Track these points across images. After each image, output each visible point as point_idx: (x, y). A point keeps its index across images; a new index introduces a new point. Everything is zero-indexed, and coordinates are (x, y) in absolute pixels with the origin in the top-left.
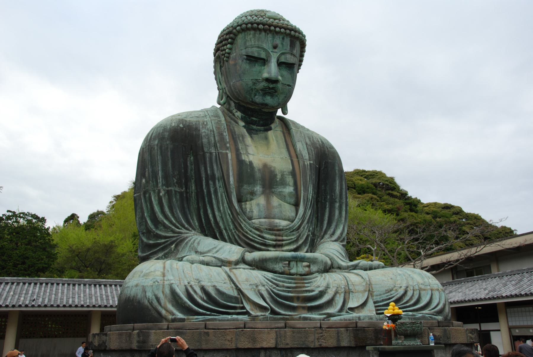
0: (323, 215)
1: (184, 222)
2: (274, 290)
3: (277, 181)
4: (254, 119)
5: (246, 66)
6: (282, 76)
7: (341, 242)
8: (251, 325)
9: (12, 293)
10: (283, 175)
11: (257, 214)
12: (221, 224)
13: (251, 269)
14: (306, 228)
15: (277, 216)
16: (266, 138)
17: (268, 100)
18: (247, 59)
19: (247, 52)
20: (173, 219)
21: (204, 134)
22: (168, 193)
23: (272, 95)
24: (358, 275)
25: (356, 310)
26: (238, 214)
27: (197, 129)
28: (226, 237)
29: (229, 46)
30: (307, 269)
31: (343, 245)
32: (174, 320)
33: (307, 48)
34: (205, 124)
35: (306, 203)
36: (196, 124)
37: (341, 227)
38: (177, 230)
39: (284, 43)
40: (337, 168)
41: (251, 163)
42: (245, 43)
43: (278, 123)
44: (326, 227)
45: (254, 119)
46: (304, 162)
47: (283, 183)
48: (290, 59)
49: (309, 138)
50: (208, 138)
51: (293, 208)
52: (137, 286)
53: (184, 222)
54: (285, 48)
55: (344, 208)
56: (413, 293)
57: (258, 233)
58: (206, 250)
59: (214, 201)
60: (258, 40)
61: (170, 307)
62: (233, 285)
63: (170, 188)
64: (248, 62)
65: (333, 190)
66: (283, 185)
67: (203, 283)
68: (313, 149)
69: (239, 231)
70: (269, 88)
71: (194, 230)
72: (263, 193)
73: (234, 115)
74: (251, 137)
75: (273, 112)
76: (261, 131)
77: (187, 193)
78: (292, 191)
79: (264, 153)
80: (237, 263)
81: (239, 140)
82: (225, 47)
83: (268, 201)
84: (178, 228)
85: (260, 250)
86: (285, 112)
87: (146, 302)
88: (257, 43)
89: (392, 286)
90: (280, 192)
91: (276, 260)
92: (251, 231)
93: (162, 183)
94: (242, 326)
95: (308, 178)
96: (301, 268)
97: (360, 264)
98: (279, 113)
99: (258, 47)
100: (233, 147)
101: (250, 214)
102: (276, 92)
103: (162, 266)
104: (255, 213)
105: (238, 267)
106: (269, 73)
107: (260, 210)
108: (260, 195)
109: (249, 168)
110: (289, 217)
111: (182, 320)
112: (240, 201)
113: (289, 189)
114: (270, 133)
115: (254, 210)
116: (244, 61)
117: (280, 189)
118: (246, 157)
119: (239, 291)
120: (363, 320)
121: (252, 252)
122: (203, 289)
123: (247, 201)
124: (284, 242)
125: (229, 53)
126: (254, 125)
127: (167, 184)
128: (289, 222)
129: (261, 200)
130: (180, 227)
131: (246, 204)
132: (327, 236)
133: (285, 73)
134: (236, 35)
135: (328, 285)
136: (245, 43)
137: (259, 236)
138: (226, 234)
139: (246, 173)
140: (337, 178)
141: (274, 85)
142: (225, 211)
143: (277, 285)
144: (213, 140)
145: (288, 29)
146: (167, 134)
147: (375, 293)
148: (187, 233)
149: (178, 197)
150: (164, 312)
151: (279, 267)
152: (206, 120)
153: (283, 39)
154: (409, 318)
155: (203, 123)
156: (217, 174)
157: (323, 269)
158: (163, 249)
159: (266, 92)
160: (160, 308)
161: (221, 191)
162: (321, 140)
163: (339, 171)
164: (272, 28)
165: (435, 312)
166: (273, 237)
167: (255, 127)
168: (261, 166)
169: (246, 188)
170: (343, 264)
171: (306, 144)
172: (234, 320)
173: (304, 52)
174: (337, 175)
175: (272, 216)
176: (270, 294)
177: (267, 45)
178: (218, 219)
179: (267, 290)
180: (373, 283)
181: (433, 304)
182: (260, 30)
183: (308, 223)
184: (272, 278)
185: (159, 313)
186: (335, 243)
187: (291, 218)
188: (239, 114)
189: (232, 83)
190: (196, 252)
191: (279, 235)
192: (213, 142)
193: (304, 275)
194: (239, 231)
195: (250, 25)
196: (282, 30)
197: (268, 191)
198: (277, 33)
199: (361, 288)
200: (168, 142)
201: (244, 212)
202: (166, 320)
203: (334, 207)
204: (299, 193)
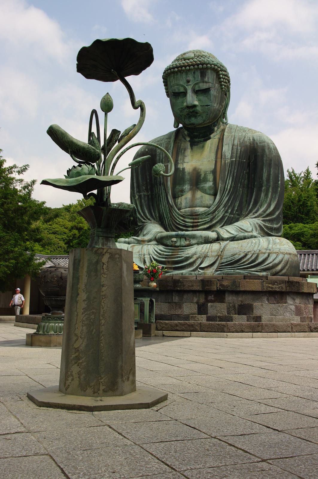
2: (155, 257)
3: (201, 179)
6: (199, 100)
7: (263, 217)
10: (205, 174)
11: (184, 205)
13: (156, 244)
14: (222, 211)
15: (198, 205)
16: (203, 147)
17: (193, 120)
18: (174, 95)
19: (172, 90)
20: (142, 214)
21: (158, 153)
22: (140, 197)
23: (196, 117)
25: (205, 270)
26: (172, 207)
28: (167, 223)
31: (263, 221)
38: (143, 220)
39: (196, 76)
40: (265, 159)
41: (184, 169)
44: (252, 207)
45: (195, 134)
47: (205, 180)
49: (239, 139)
51: (212, 197)
54: (196, 79)
55: (271, 190)
56: (252, 256)
57: (182, 218)
63: (140, 194)
68: (239, 148)
69: (173, 219)
70: (192, 112)
71: (154, 219)
72: (191, 189)
74: (192, 149)
75: (209, 126)
76: (201, 142)
78: (212, 185)
79: (198, 160)
80: (150, 241)
81: (181, 153)
83: (193, 195)
89: (238, 252)
92: (178, 218)
93: (137, 191)
95: (227, 173)
97: (237, 236)
99: (178, 85)
102: (197, 113)
104: (183, 204)
105: (149, 243)
106: (187, 102)
108: (188, 192)
109: (181, 173)
112: (175, 197)
113: (210, 184)
114: (209, 142)
115: (183, 203)
117: (202, 185)
120: (185, 275)
123: (179, 197)
124: (199, 224)
126: (196, 138)
127: (139, 192)
130: (146, 219)
133: (201, 97)
135: (195, 252)
138: (167, 221)
139: (179, 177)
141: (194, 109)
142: (166, 206)
143: (160, 254)
144: (161, 157)
148: (147, 222)
149: (146, 199)
153: (194, 73)
154: (224, 274)
157: (203, 242)
161: (163, 192)
164: (183, 68)
166: (192, 221)
167: (197, 140)
168: (191, 170)
169: (178, 188)
171: (233, 145)
175: (195, 205)
177: (182, 82)
179: (150, 258)
180: (226, 250)
181: (265, 263)
182: (177, 72)
183: (225, 206)
186: (254, 219)
187: (209, 205)
188: (186, 132)
191: (196, 219)
192: (161, 158)
193: (185, 246)
197: (194, 188)
199: (215, 254)
204: (218, 185)
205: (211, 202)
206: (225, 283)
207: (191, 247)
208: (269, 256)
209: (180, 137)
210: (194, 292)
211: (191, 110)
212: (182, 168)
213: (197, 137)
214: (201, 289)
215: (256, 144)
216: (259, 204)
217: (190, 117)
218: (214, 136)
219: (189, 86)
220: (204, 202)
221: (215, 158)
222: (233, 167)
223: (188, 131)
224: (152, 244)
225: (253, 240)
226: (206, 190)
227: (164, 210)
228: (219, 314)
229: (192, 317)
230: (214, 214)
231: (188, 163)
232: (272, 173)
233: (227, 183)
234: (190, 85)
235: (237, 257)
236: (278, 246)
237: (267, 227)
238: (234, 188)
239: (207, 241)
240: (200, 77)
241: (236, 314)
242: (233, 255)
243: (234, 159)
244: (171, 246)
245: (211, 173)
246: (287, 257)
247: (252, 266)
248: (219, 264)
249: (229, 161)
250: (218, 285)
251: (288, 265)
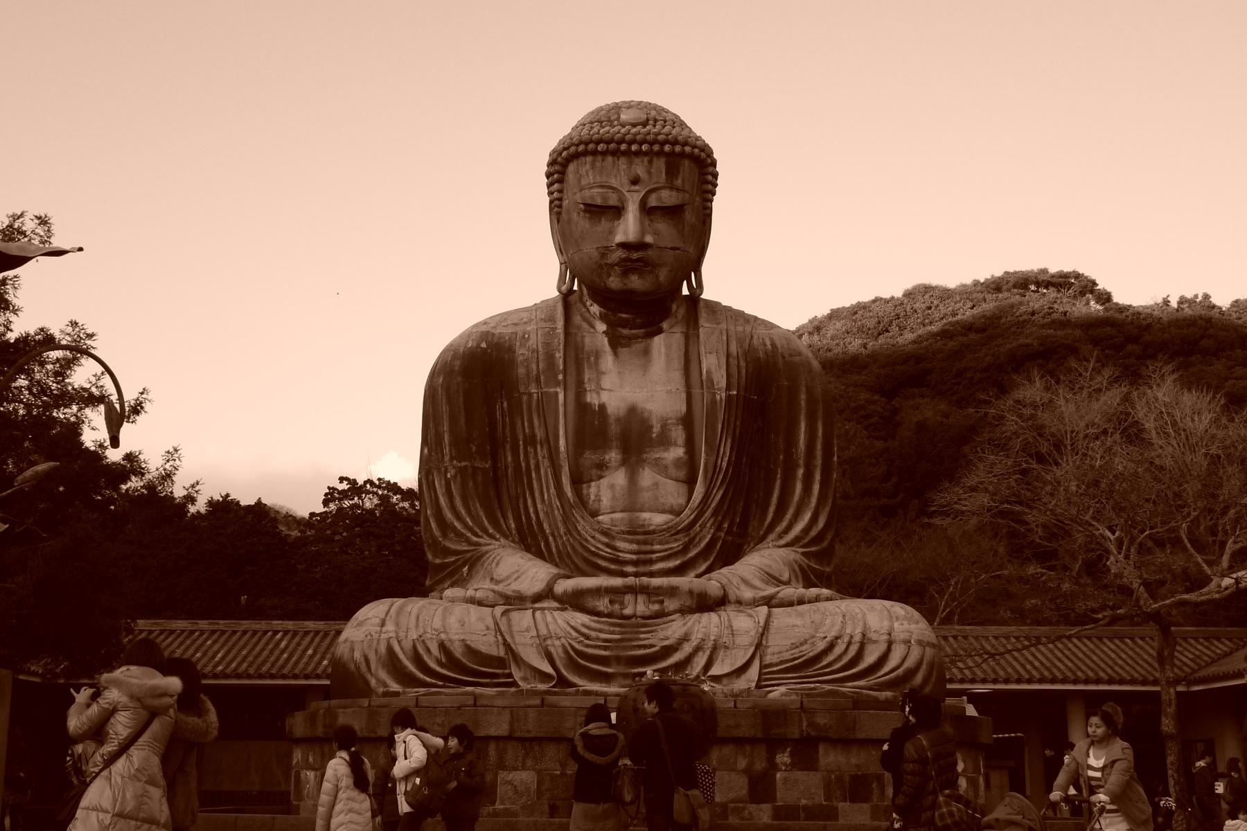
0: (770, 495)
1: (486, 523)
4: (624, 316)
6: (656, 233)
7: (802, 547)
8: (485, 702)
9: (310, 652)
10: (664, 426)
12: (546, 526)
13: (558, 609)
16: (646, 352)
18: (585, 211)
22: (461, 471)
23: (641, 275)
24: (751, 616)
25: (725, 681)
27: (511, 350)
28: (554, 550)
30: (656, 607)
31: (803, 554)
32: (386, 694)
34: (525, 339)
35: (709, 475)
37: (807, 516)
38: (475, 539)
40: (803, 396)
41: (602, 407)
43: (680, 316)
46: (714, 394)
47: (665, 441)
48: (668, 197)
49: (740, 342)
50: (527, 367)
51: (683, 489)
52: (346, 641)
53: (486, 523)
54: (655, 180)
55: (818, 477)
58: (505, 575)
59: (535, 485)
61: (383, 675)
62: (500, 638)
63: (463, 464)
65: (791, 442)
67: (443, 636)
68: (743, 364)
69: (575, 538)
71: (506, 537)
72: (624, 462)
74: (616, 354)
76: (637, 337)
77: (495, 468)
81: (588, 361)
84: (477, 535)
85: (584, 574)
87: (352, 667)
89: (807, 637)
91: (597, 592)
94: (471, 702)
96: (641, 606)
97: (780, 595)
99: (602, 187)
100: (571, 380)
101: (596, 506)
103: (386, 608)
104: (606, 502)
105: (537, 605)
106: (625, 233)
107: (614, 498)
108: (617, 468)
111: (396, 694)
113: (678, 452)
114: (658, 342)
118: (595, 395)
119: (507, 646)
121: (569, 577)
122: (442, 646)
123: (591, 480)
125: (560, 199)
126: (624, 327)
128: (670, 517)
129: (619, 478)
131: (589, 487)
132: (772, 536)
133: (662, 226)
134: (565, 165)
137: (607, 545)
138: (553, 545)
139: (593, 428)
140: (803, 417)
142: (550, 503)
143: (587, 637)
146: (457, 363)
147: (770, 650)
149: (480, 479)
150: (373, 682)
151: (603, 604)
153: (650, 162)
154: (797, 694)
156: (540, 434)
158: (452, 574)
159: (627, 268)
160: (369, 676)
161: (545, 464)
162: (772, 340)
163: (808, 401)
165: (876, 684)
166: (634, 547)
167: (625, 332)
168: (622, 412)
169: (589, 457)
170: (748, 594)
171: (728, 356)
172: (467, 694)
174: (803, 412)
175: (638, 506)
176: (566, 652)
178: (542, 515)
180: (772, 631)
182: (604, 153)
183: (716, 513)
184: (583, 625)
185: (367, 683)
187: (676, 508)
188: (595, 309)
190: (492, 579)
191: (645, 543)
192: (535, 373)
194: (575, 538)
195: (581, 148)
196: (644, 147)
198: (639, 153)
200: (459, 379)
201: (582, 500)
202: (378, 696)
203: (794, 477)
206: (821, 720)
207: (665, 619)
208: (889, 649)
209: (577, 319)
210: (740, 742)
211: (635, 256)
213: (625, 323)
214: (760, 735)
215: (780, 359)
216: (791, 511)
217: (626, 273)
218: (671, 327)
220: (662, 500)
222: (733, 412)
224: (549, 609)
225: (821, 605)
226: (666, 467)
227: (546, 513)
228: (804, 802)
229: (734, 809)
230: (692, 533)
232: (820, 433)
235: (810, 651)
236: (906, 626)
237: (813, 570)
238: (735, 464)
239: (705, 604)
241: (845, 801)
242: (795, 646)
244: (609, 615)
246: (929, 652)
247: (854, 674)
248: (761, 667)
249: (724, 395)
250: (805, 724)
251: (935, 674)
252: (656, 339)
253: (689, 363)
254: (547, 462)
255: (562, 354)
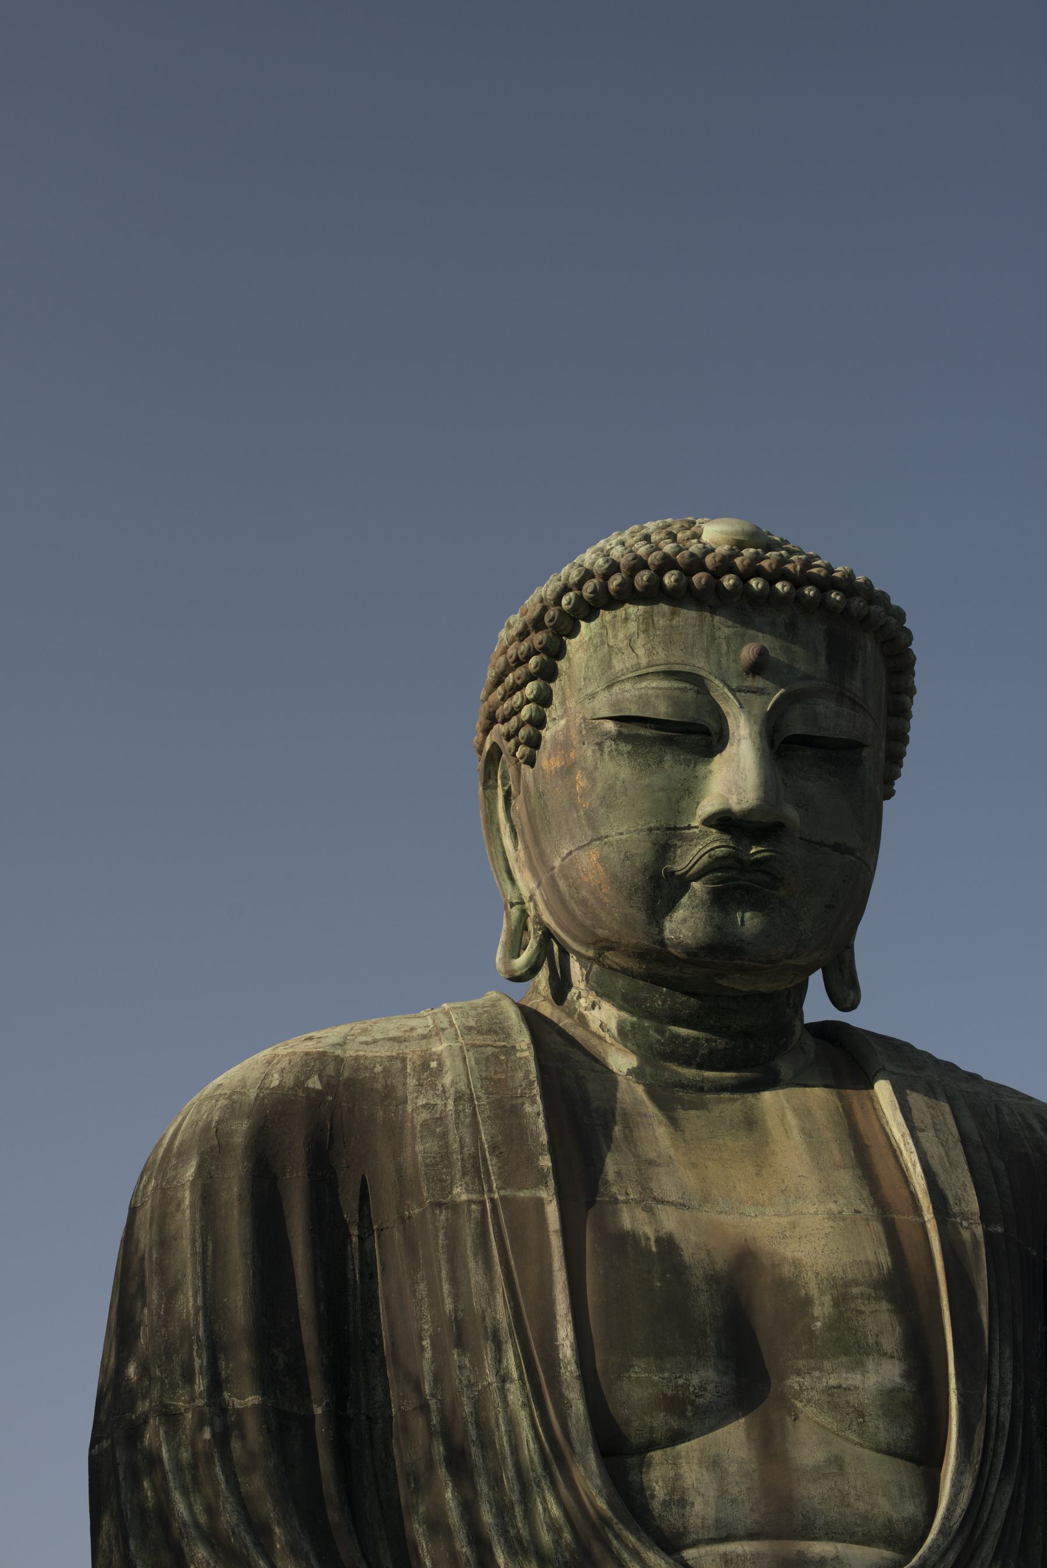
3: (811, 1334)
4: (683, 1031)
5: (617, 769)
10: (841, 1301)
11: (711, 1513)
16: (751, 1123)
18: (619, 737)
19: (615, 704)
21: (424, 1115)
27: (391, 1096)
29: (530, 689)
33: (922, 677)
34: (428, 1070)
36: (386, 1071)
41: (668, 1245)
42: (607, 664)
47: (847, 1343)
50: (444, 1136)
60: (668, 642)
64: (625, 748)
66: (847, 1352)
73: (583, 1021)
74: (674, 1123)
76: (720, 1088)
78: (898, 1380)
82: (517, 698)
83: (770, 1446)
86: (845, 991)
88: (661, 655)
90: (830, 1390)
98: (817, 1006)
99: (669, 674)
104: (702, 1509)
107: (722, 1492)
110: (889, 1523)
116: (608, 743)
118: (641, 1215)
123: (653, 1445)
126: (687, 1063)
128: (887, 1554)
131: (649, 1465)
136: (607, 664)
144: (468, 1139)
145: (811, 580)
152: (439, 1047)
155: (425, 1066)
167: (690, 1073)
173: (911, 691)
189: (557, 863)
205: (911, 1509)
212: (659, 1240)
219: (756, 700)
220: (861, 1506)
221: (866, 1193)
223: (626, 1002)
231: (687, 1213)
233: (996, 1381)
234: (760, 692)
240: (823, 659)
243: (999, 1229)
245: (878, 1299)
249: (979, 1230)
252: (767, 1096)
253: (864, 1154)
254: (515, 1394)
255: (539, 1106)
